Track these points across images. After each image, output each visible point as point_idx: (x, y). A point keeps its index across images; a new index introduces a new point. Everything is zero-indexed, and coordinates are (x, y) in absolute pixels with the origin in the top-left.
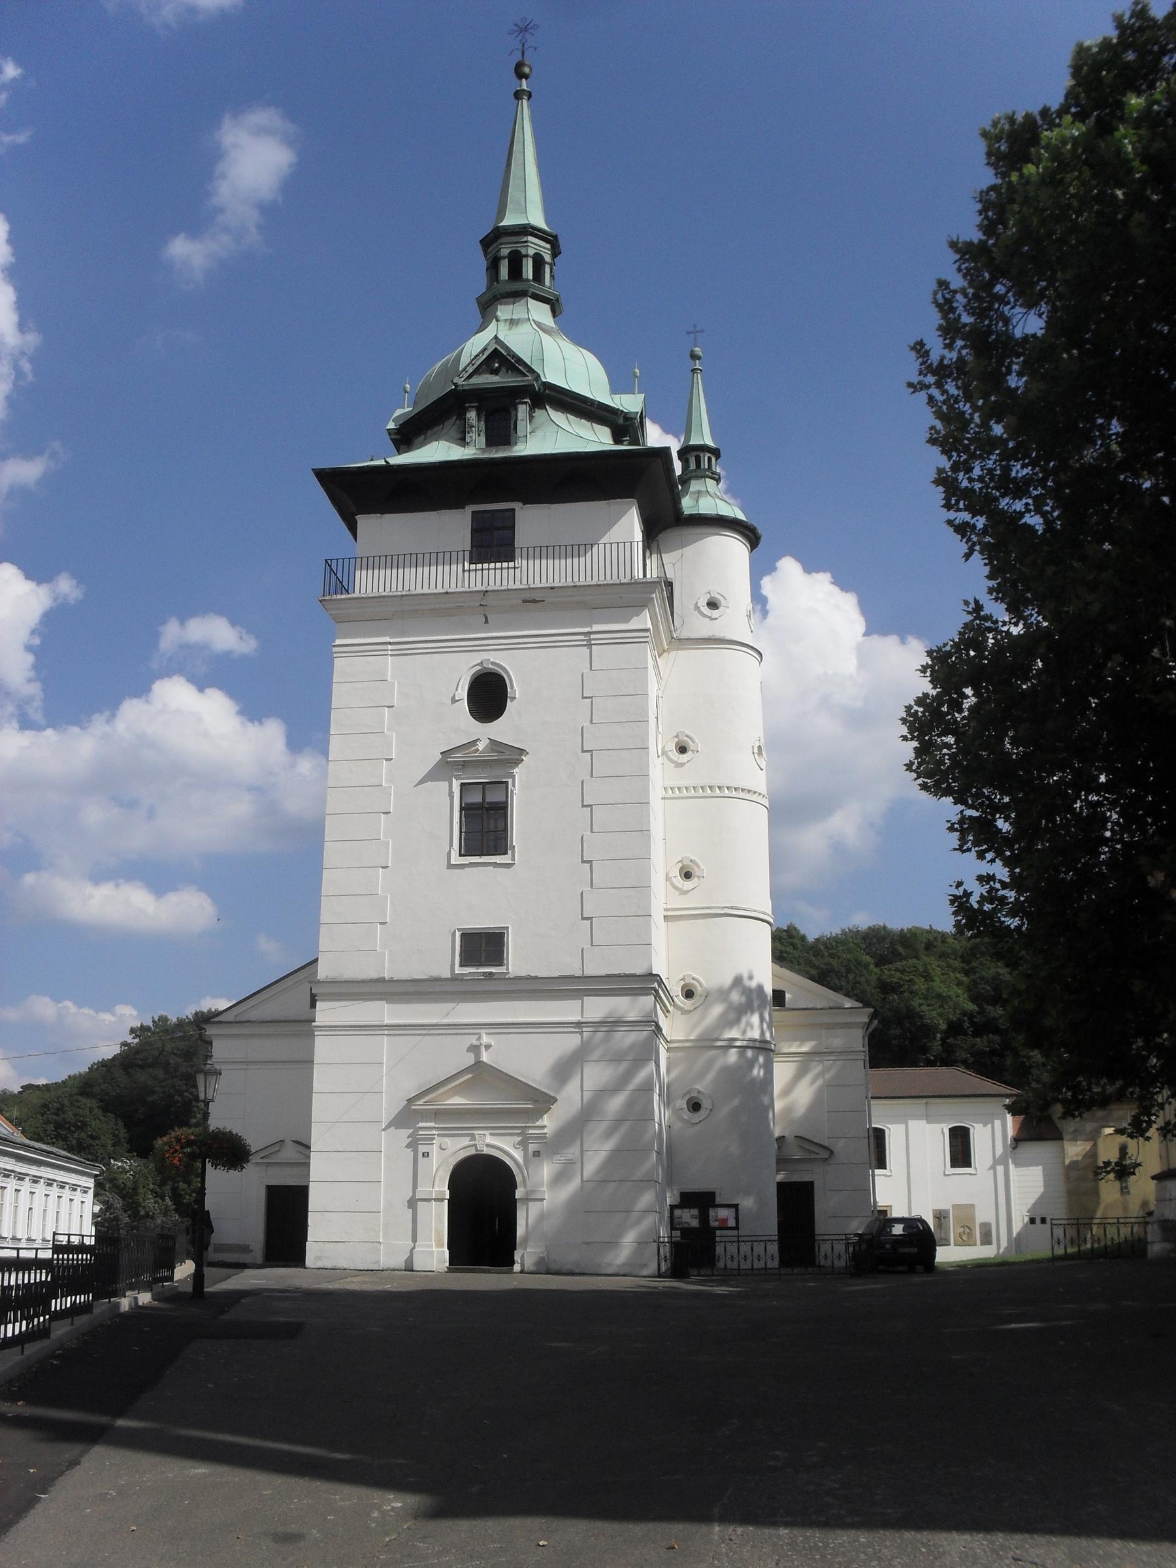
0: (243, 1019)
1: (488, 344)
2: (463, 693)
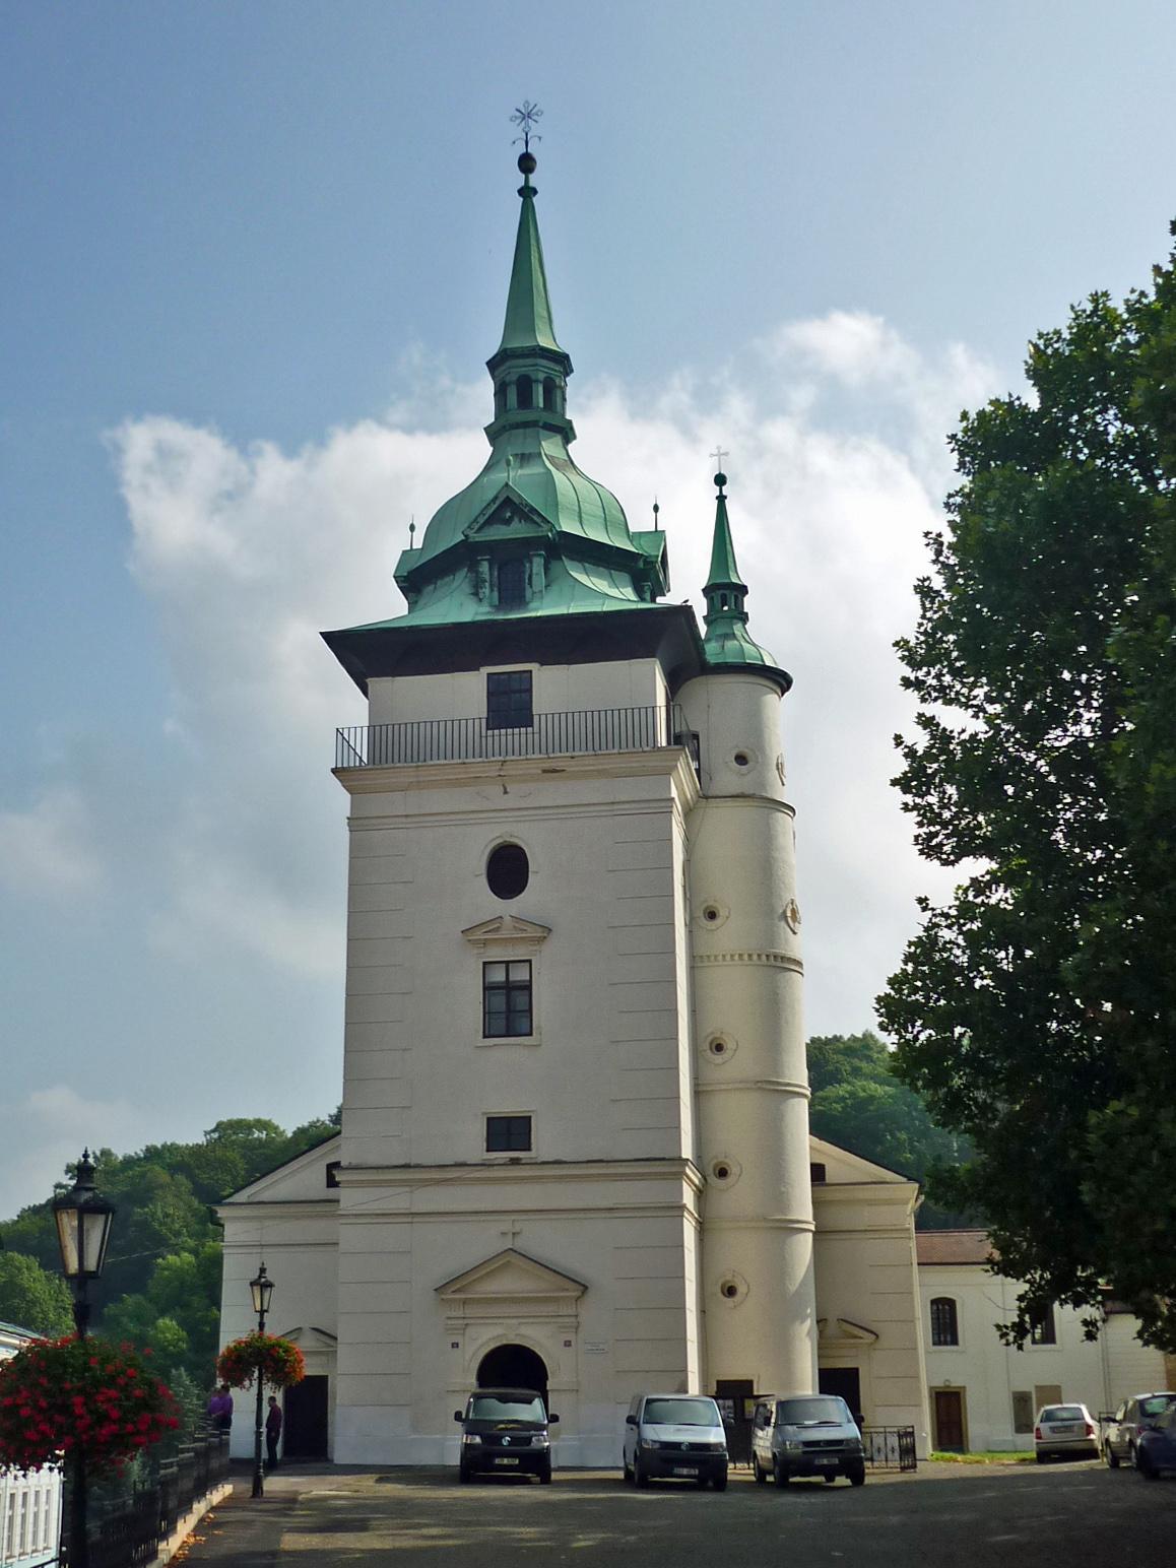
0: (257, 1200)
1: (499, 493)
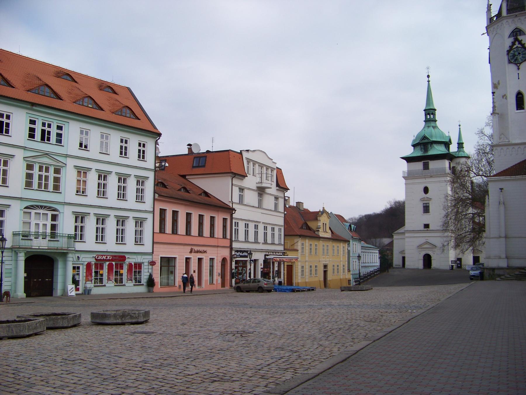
2: (423, 190)
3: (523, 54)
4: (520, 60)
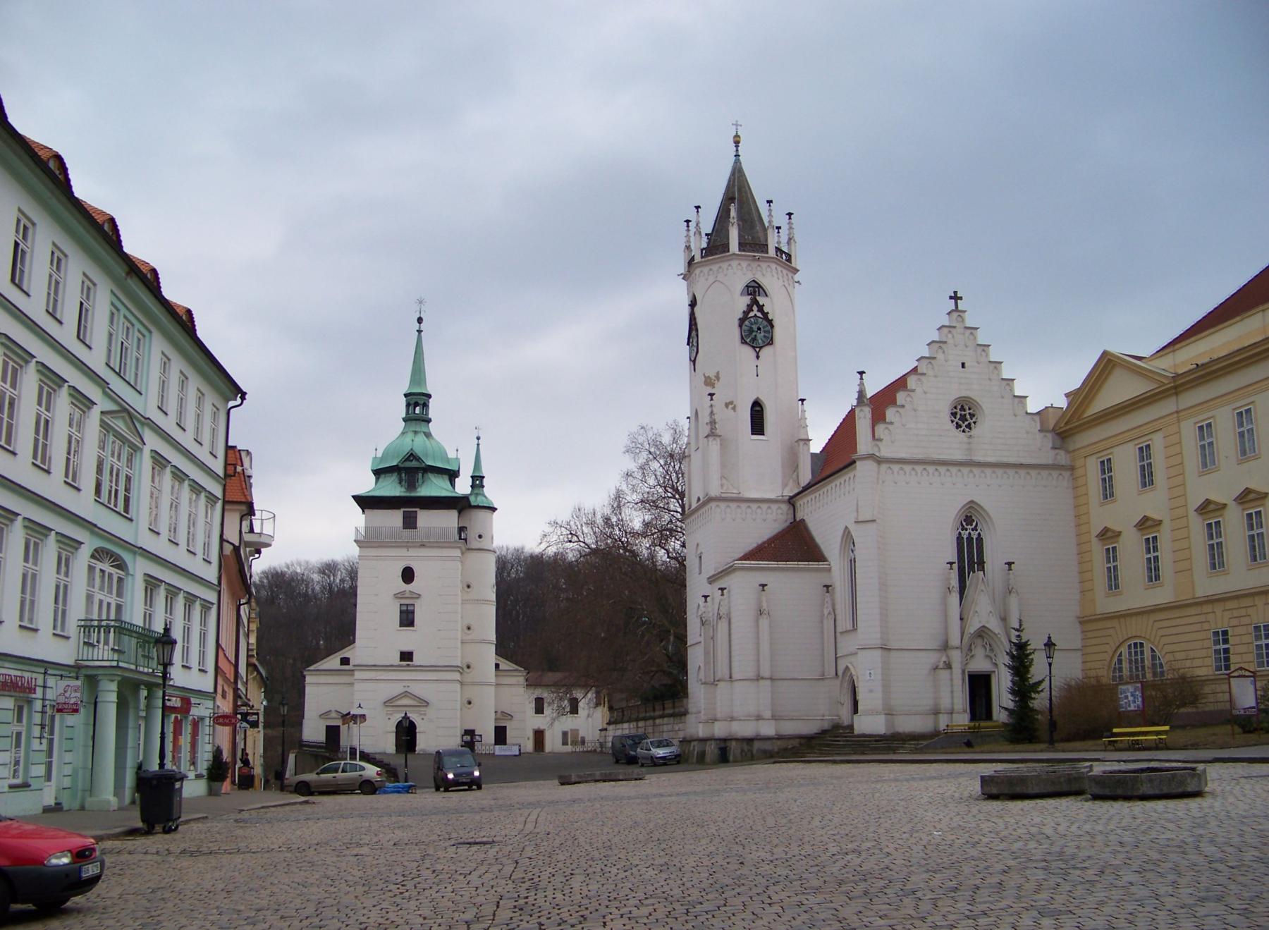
3: (765, 332)
4: (760, 341)
